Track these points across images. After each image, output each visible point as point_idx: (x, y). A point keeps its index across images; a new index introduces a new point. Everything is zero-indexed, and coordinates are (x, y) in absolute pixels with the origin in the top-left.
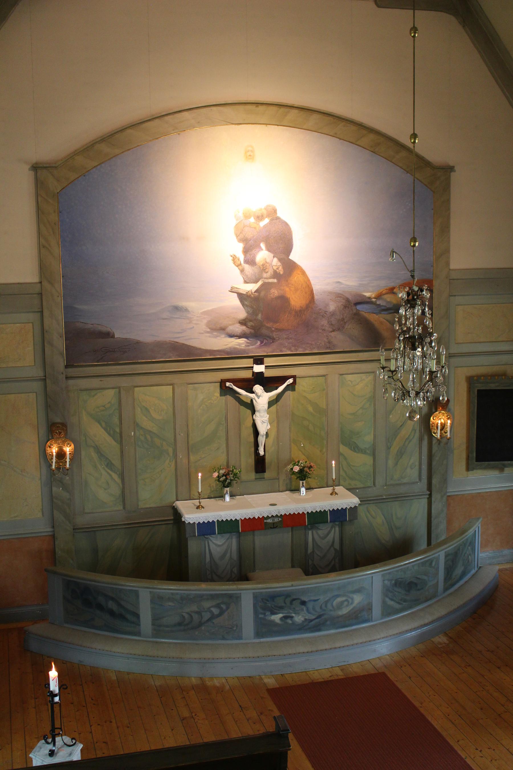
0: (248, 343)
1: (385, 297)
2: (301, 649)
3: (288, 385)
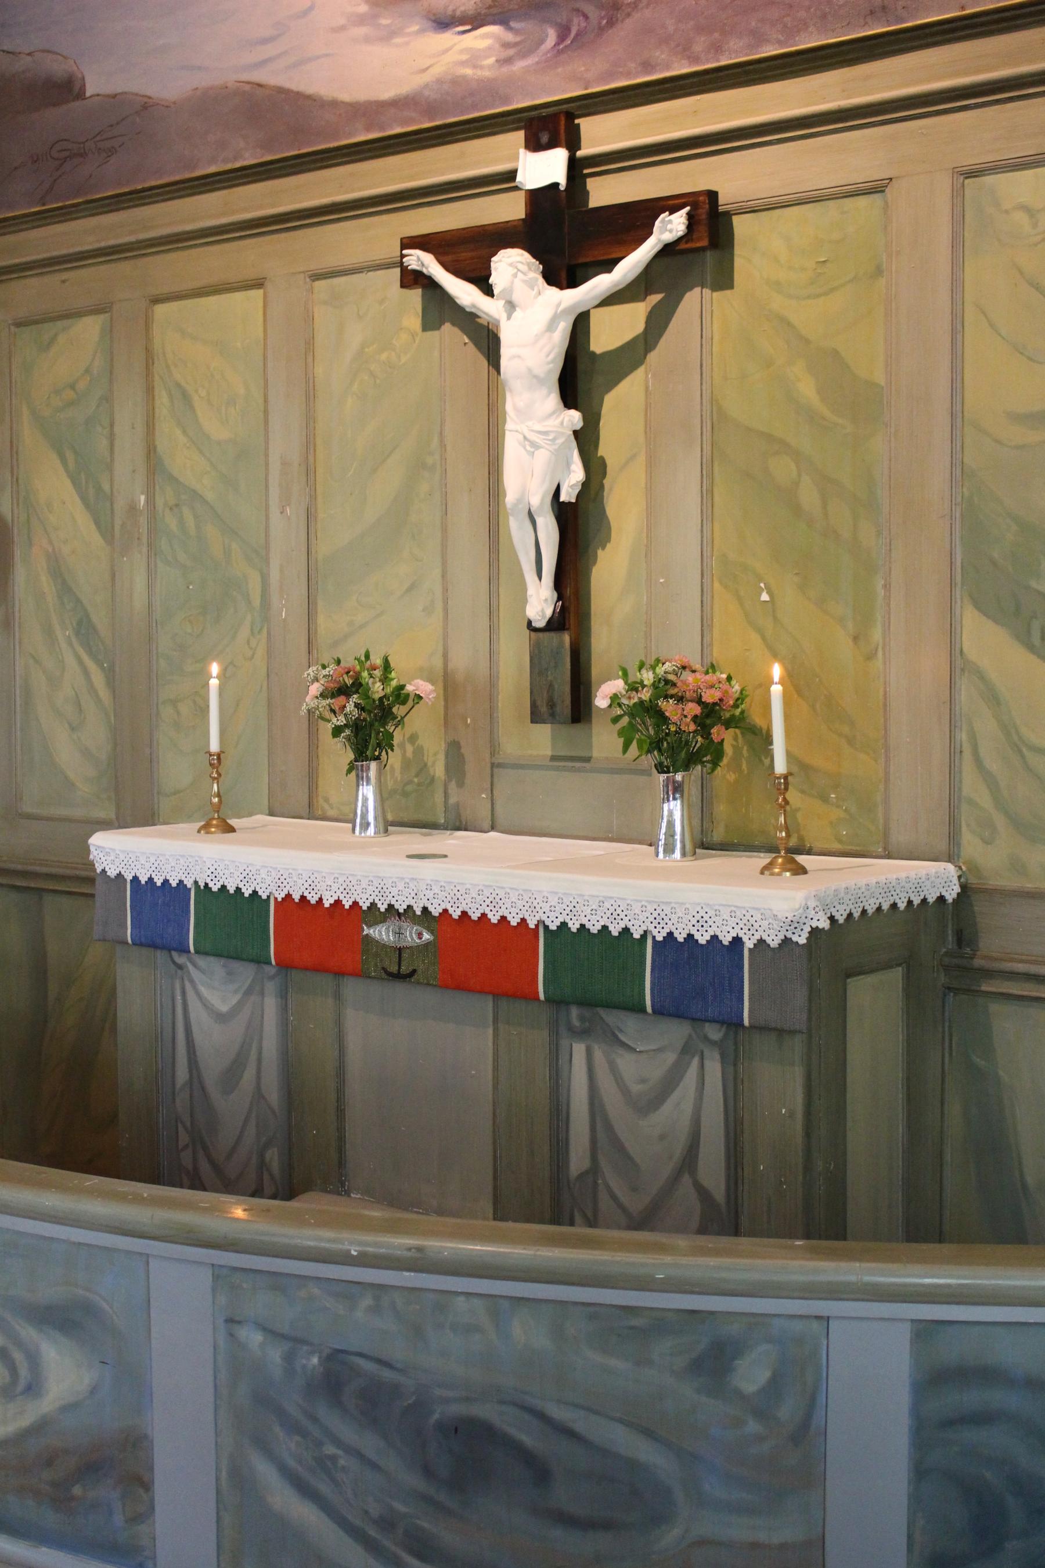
0: (506, 45)
3: (668, 250)
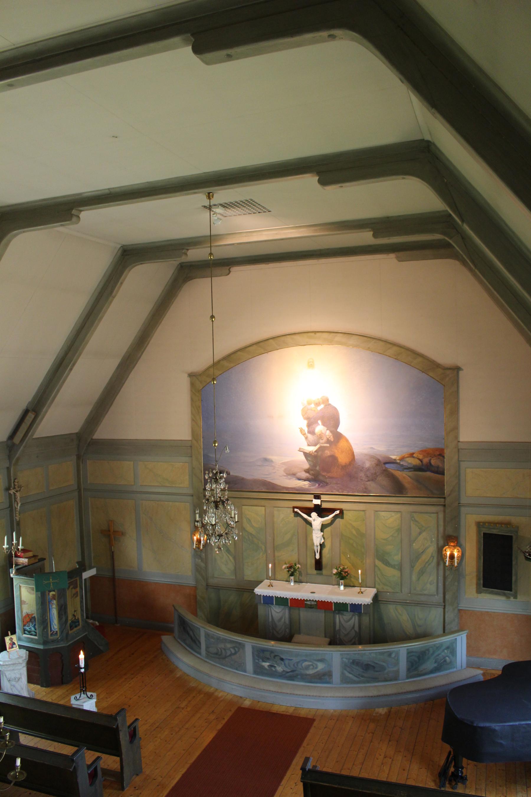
1: (407, 459)
2: (272, 688)
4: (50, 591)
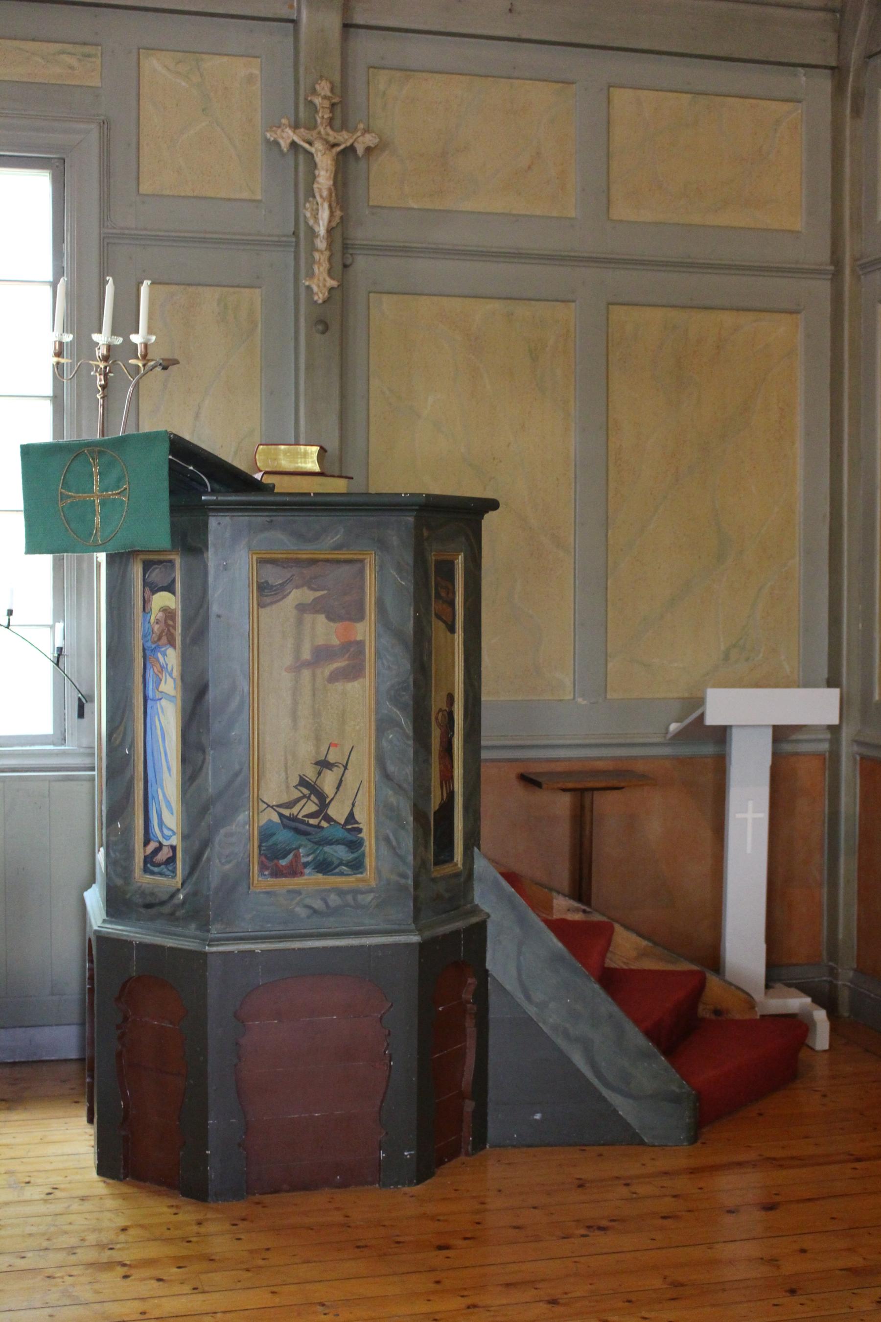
4: (155, 589)
